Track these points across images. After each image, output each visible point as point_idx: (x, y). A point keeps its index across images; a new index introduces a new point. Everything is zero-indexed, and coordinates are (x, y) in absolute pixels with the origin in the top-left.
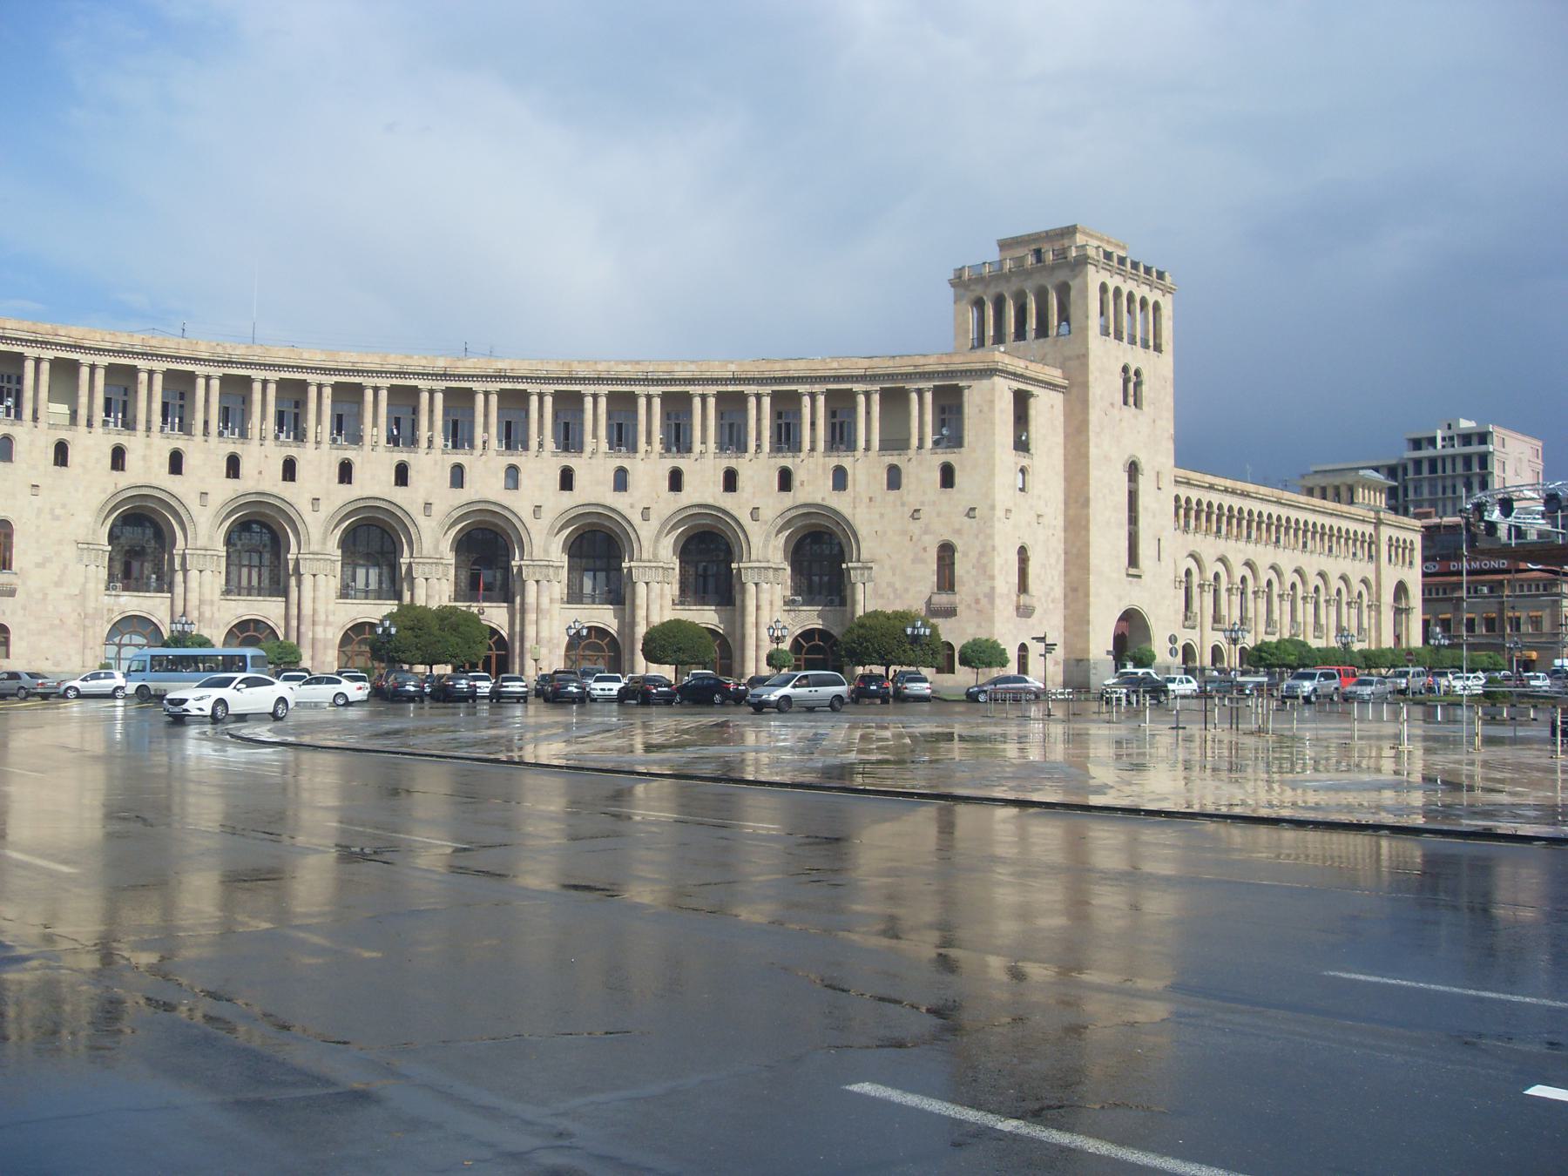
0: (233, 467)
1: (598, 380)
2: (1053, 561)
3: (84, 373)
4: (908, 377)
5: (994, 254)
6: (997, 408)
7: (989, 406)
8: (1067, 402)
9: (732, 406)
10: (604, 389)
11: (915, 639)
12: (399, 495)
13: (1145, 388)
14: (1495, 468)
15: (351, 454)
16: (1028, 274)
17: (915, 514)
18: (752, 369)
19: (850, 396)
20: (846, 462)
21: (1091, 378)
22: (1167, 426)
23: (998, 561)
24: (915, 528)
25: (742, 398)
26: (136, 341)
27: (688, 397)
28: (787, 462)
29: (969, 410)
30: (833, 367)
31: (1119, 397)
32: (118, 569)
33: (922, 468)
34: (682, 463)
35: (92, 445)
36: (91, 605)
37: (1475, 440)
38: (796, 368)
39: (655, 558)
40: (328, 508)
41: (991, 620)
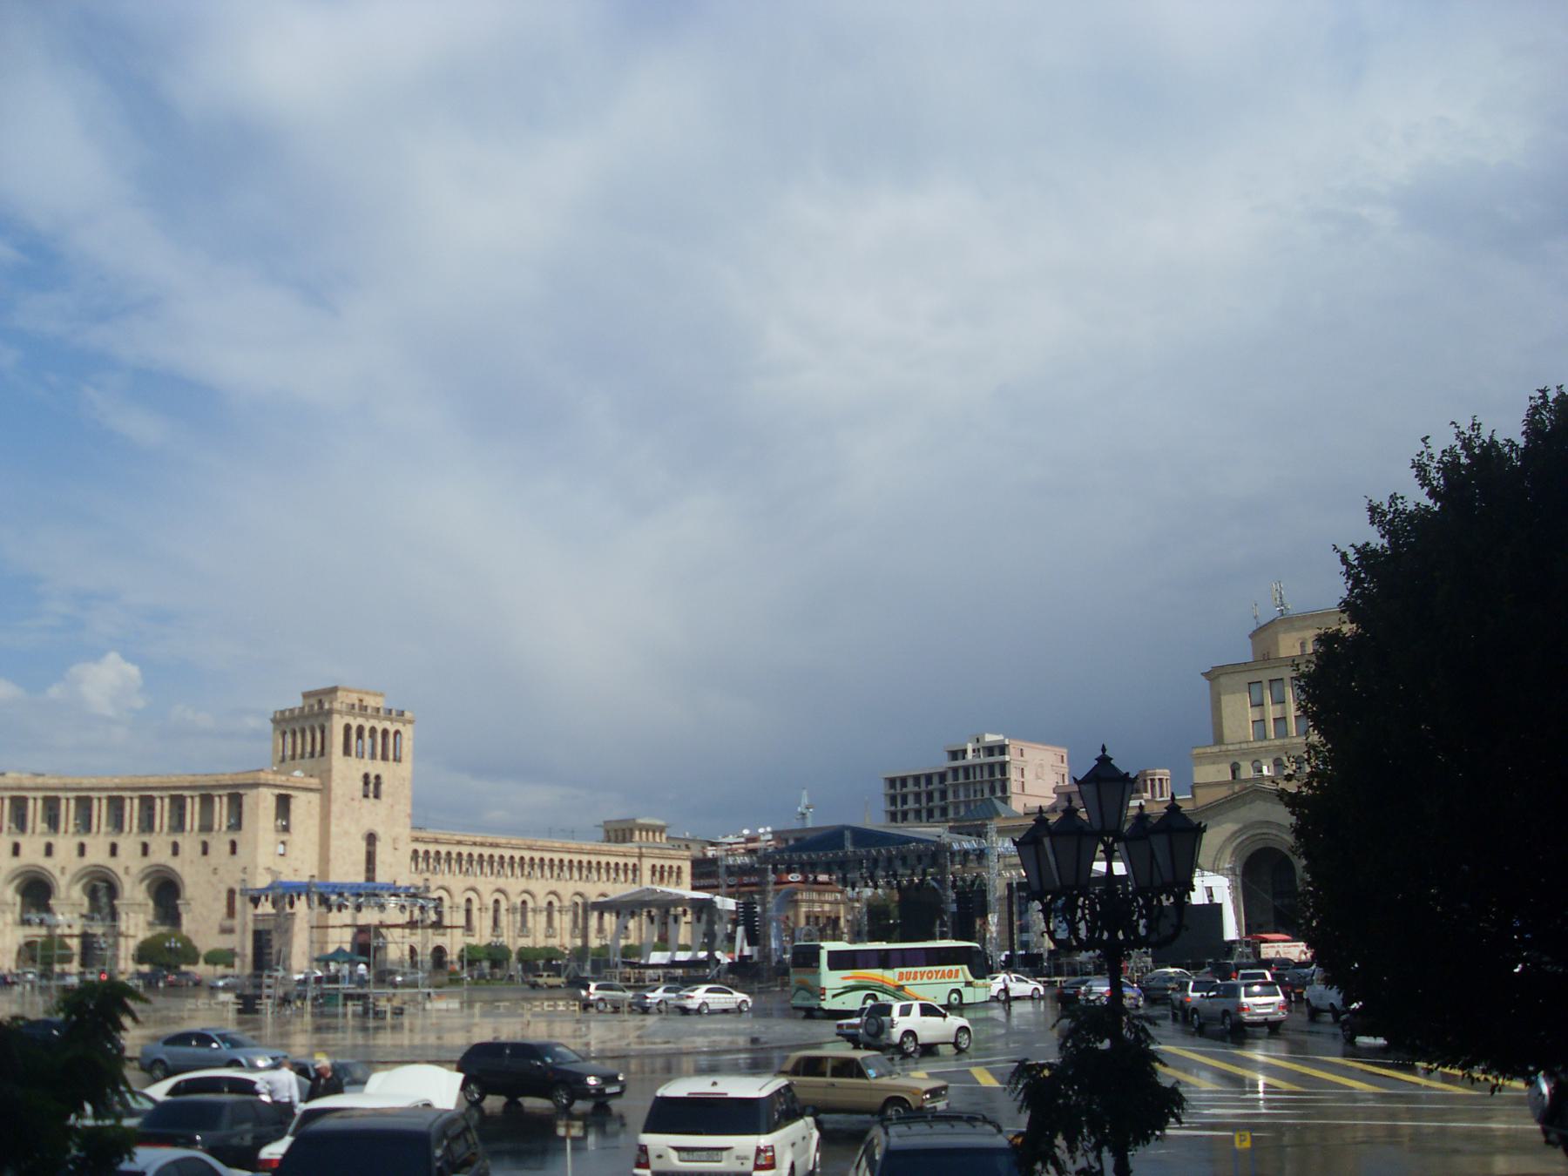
5: (297, 702)
6: (262, 805)
7: (262, 804)
8: (322, 800)
9: (116, 805)
10: (40, 794)
11: (170, 949)
13: (384, 787)
14: (1013, 775)
16: (306, 718)
17: (215, 871)
18: (127, 782)
19: (183, 798)
20: (179, 838)
21: (334, 785)
22: (404, 807)
24: (214, 879)
25: (122, 799)
27: (90, 799)
29: (246, 808)
30: (174, 781)
31: (360, 794)
33: (219, 843)
34: (86, 840)
37: (996, 751)
38: (153, 781)
39: (68, 897)
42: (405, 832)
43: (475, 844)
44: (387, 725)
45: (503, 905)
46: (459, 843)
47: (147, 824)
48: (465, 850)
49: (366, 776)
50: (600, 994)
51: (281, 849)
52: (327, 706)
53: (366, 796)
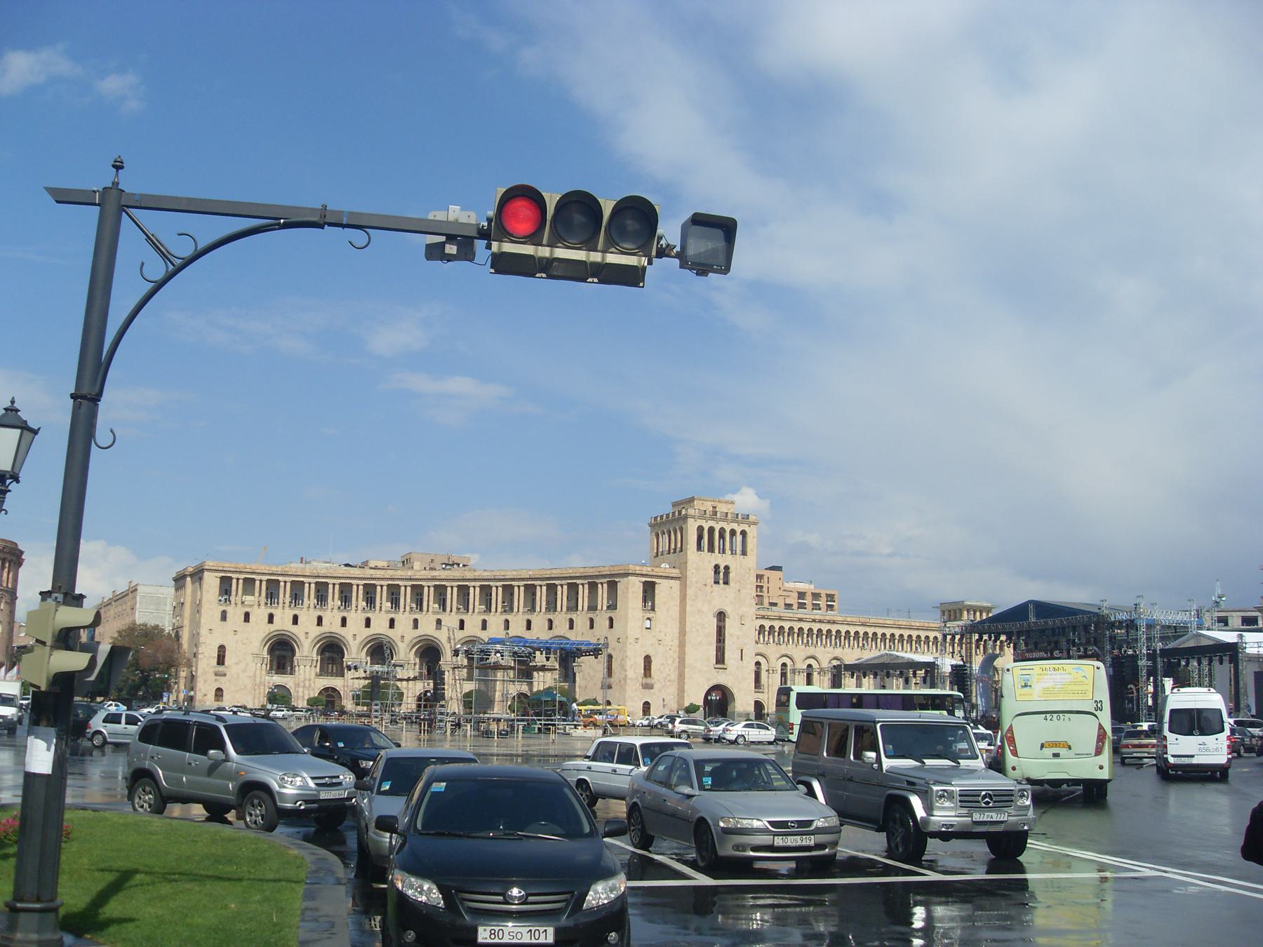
0: (320, 621)
1: (475, 580)
2: (670, 662)
3: (258, 583)
4: (597, 577)
5: (670, 510)
6: (630, 590)
7: (632, 590)
9: (530, 590)
12: (390, 633)
15: (369, 615)
20: (574, 617)
23: (629, 663)
26: (279, 570)
27: (512, 587)
28: (551, 617)
30: (570, 572)
32: (275, 663)
33: (601, 619)
34: (509, 617)
35: (259, 614)
36: (258, 680)
38: (555, 573)
40: (359, 639)
41: (625, 690)
42: (750, 609)
43: (814, 621)
44: (735, 526)
45: (764, 667)
46: (800, 620)
47: (552, 606)
48: (806, 626)
49: (717, 567)
50: (684, 727)
51: (648, 624)
52: (684, 512)
53: (717, 582)
